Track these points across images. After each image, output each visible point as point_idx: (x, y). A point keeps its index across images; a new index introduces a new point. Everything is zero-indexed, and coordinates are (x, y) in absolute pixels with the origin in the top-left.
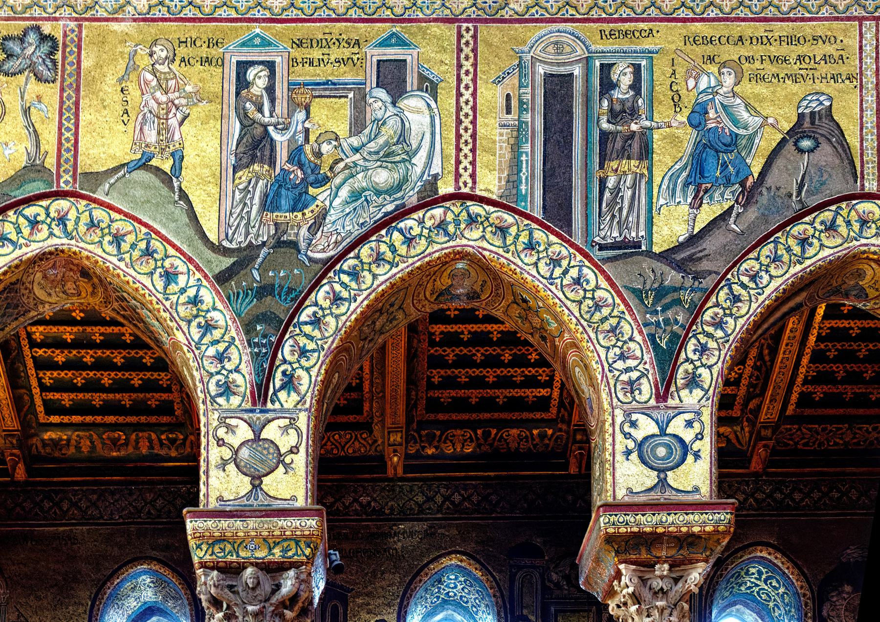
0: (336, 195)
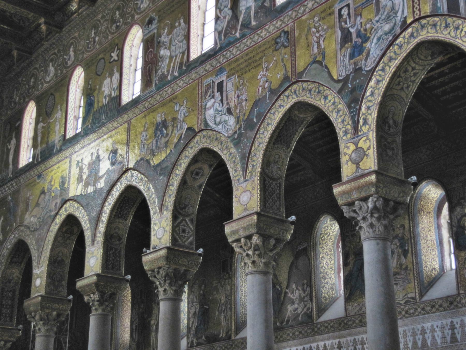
0: (372, 42)
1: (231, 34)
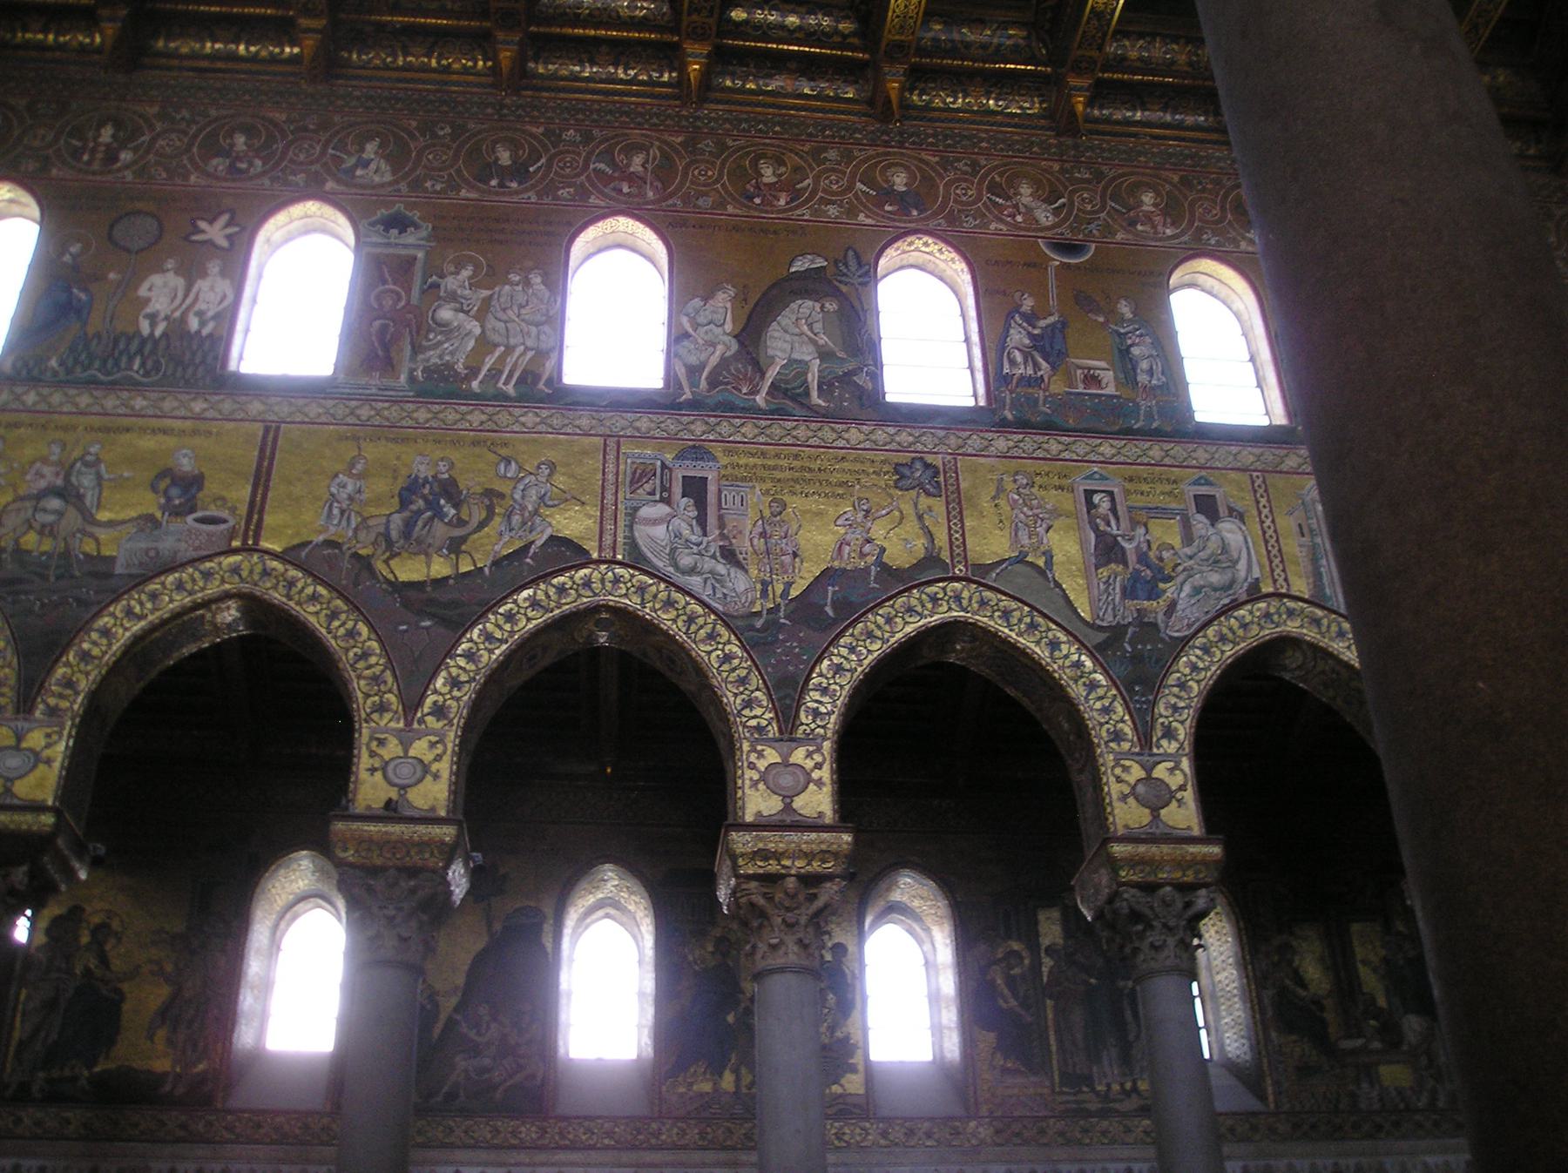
0: (1181, 590)
1: (740, 391)
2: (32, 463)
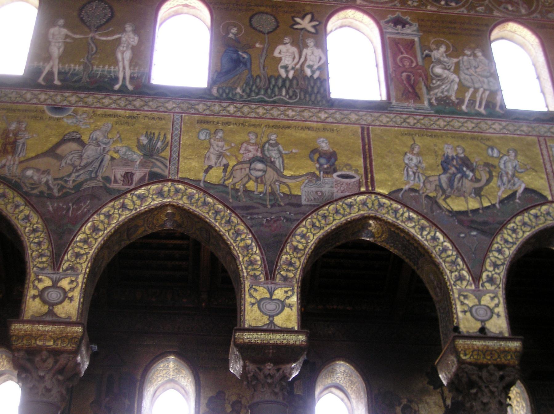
2: (242, 144)
